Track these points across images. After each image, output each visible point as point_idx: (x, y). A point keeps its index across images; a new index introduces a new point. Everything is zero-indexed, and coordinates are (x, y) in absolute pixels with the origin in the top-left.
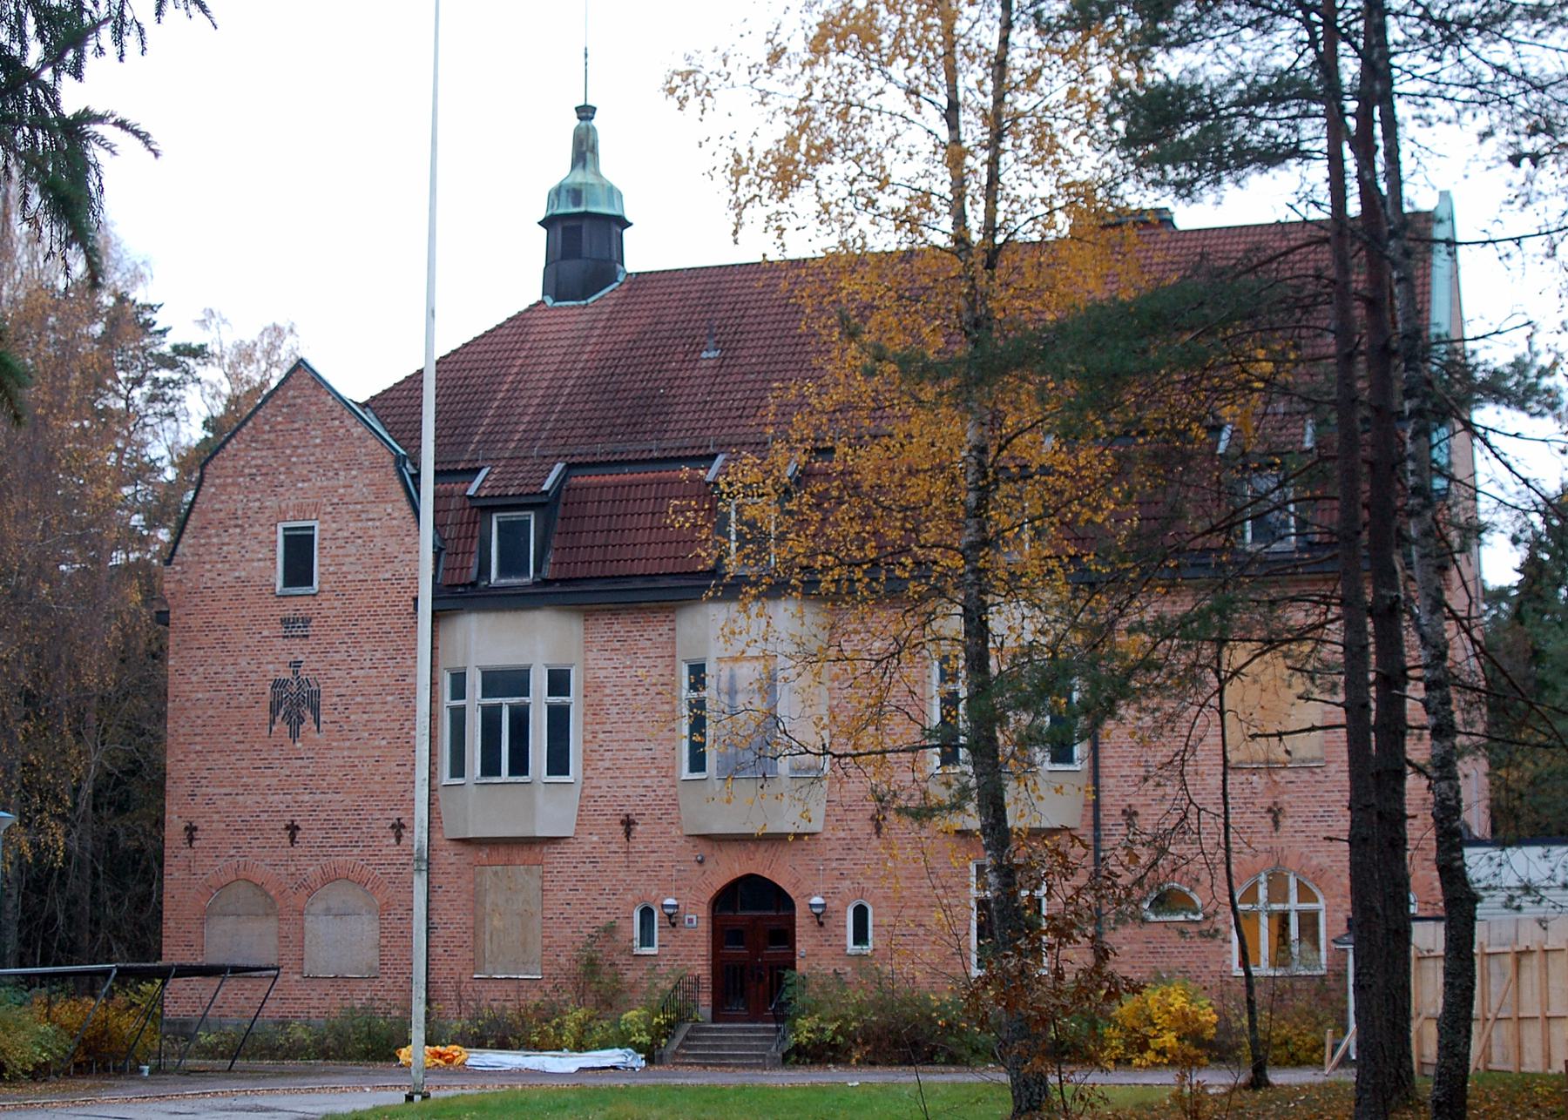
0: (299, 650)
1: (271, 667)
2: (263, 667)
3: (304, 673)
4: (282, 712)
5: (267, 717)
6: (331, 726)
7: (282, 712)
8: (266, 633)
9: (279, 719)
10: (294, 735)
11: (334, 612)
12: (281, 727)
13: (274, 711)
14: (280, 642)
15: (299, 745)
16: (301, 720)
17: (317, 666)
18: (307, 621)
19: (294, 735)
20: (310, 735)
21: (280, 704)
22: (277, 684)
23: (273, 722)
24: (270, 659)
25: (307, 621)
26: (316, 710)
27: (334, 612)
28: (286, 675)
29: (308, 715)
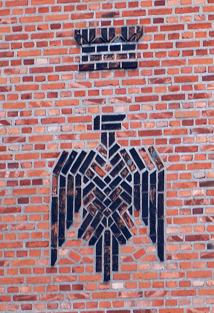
0: (114, 93)
1: (53, 128)
2: (38, 130)
3: (124, 138)
4: (79, 219)
5: (45, 228)
6: (186, 247)
7: (79, 219)
8: (41, 61)
9: (71, 233)
10: (107, 266)
11: (192, 17)
12: (78, 250)
13: (60, 216)
14: (72, 81)
15: (117, 285)
16: (122, 234)
17: (158, 124)
18: (131, 37)
19: (107, 266)
20: (143, 265)
21: (74, 204)
22: (69, 163)
23: (59, 239)
24: (51, 112)
25: (131, 37)
26: (154, 216)
27: (192, 17)
28: (86, 142)
29: (138, 224)
